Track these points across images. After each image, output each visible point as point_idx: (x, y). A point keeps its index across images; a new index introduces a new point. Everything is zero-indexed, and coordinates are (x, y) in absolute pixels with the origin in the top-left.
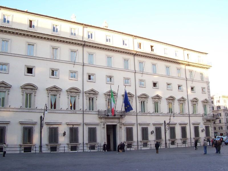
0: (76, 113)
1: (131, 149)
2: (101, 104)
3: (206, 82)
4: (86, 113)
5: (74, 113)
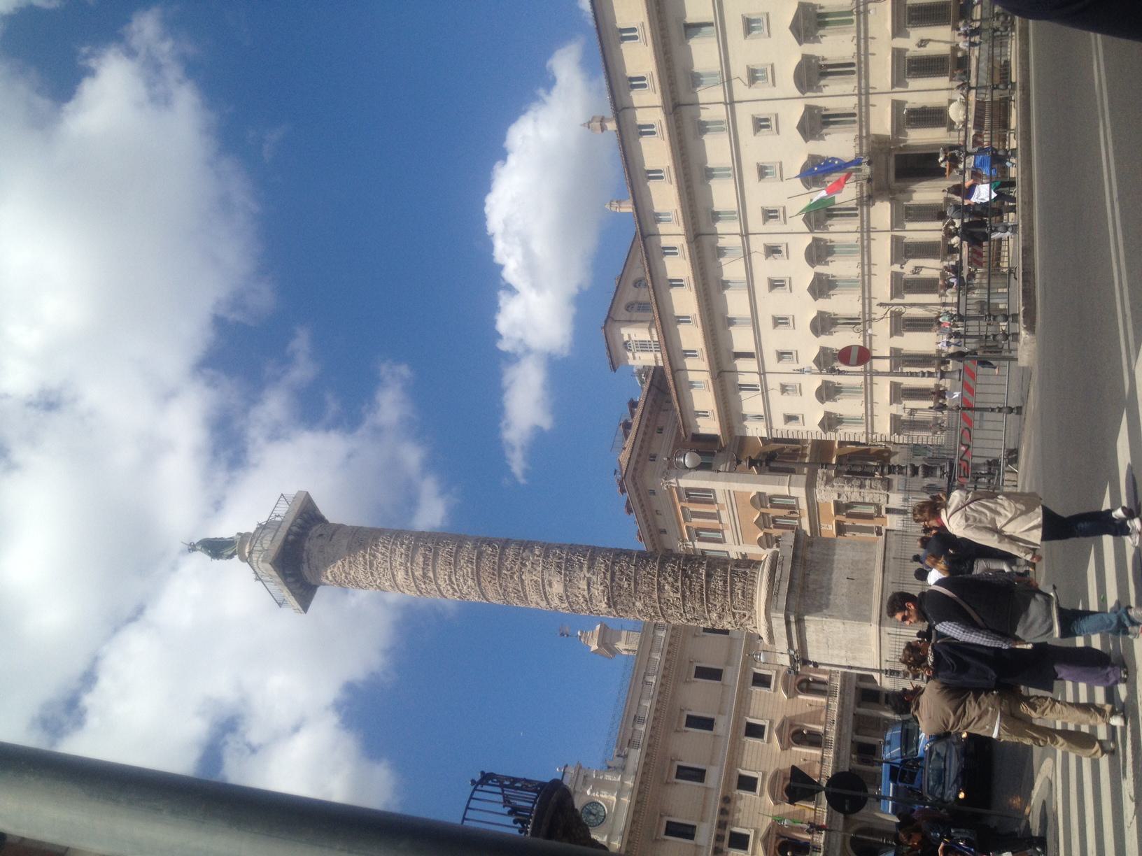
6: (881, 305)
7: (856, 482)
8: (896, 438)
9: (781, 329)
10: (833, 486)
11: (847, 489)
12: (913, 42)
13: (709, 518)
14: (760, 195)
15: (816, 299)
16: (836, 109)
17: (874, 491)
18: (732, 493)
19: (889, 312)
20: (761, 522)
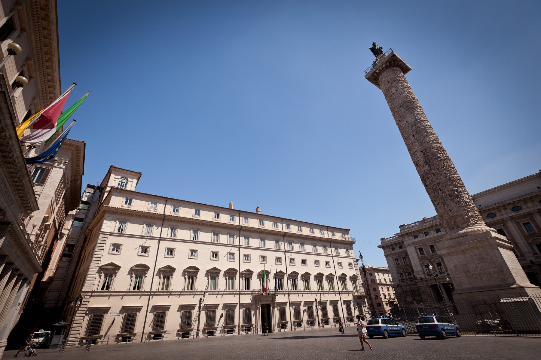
1: (286, 330)
2: (256, 284)
14: (255, 255)
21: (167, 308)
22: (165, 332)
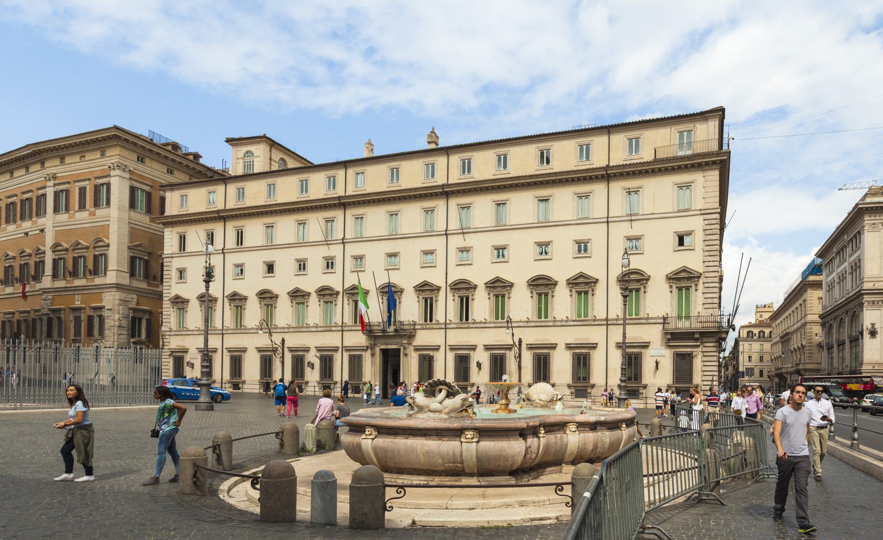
0: (330, 331)
3: (700, 210)
4: (346, 329)
5: (327, 331)
6: (283, 341)
7: (125, 323)
8: (166, 353)
9: (266, 268)
10: (119, 305)
11: (117, 316)
12: (481, 357)
13: (80, 202)
14: (375, 254)
15: (288, 293)
16: (437, 308)
17: (116, 337)
18: (107, 223)
19: (277, 346)
20: (80, 246)
21: (244, 350)
22: (244, 382)
